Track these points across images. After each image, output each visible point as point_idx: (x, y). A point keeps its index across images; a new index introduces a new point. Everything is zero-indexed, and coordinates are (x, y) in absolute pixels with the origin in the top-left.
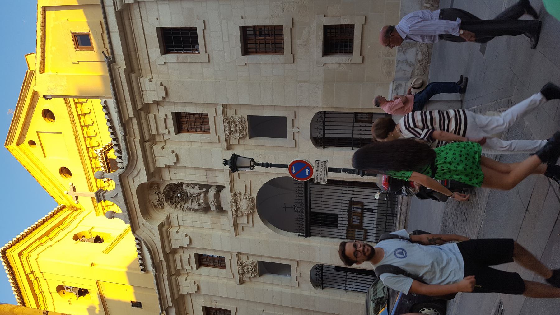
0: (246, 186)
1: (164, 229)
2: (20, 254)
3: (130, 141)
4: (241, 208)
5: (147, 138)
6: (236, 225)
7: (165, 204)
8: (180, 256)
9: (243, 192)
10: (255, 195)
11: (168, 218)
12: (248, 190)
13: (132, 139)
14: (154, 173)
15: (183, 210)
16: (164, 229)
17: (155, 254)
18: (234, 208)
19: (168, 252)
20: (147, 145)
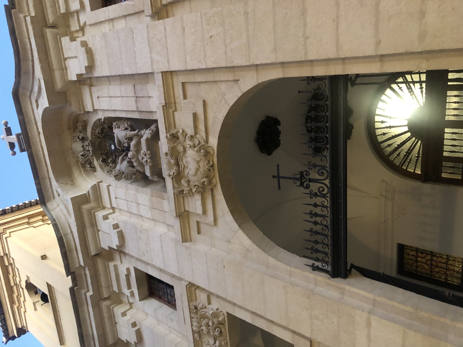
0: (195, 116)
1: (86, 208)
2: (10, 233)
3: (18, 18)
4: (186, 172)
5: (51, 18)
6: (183, 215)
7: (96, 163)
8: (115, 267)
9: (190, 131)
10: (214, 142)
11: (96, 188)
12: (202, 127)
13: (22, 16)
14: (64, 95)
15: (118, 177)
16: (86, 208)
17: (71, 251)
18: (174, 170)
19: (93, 253)
20: (49, 32)
